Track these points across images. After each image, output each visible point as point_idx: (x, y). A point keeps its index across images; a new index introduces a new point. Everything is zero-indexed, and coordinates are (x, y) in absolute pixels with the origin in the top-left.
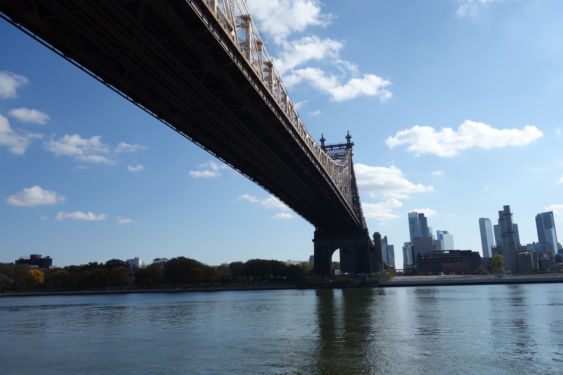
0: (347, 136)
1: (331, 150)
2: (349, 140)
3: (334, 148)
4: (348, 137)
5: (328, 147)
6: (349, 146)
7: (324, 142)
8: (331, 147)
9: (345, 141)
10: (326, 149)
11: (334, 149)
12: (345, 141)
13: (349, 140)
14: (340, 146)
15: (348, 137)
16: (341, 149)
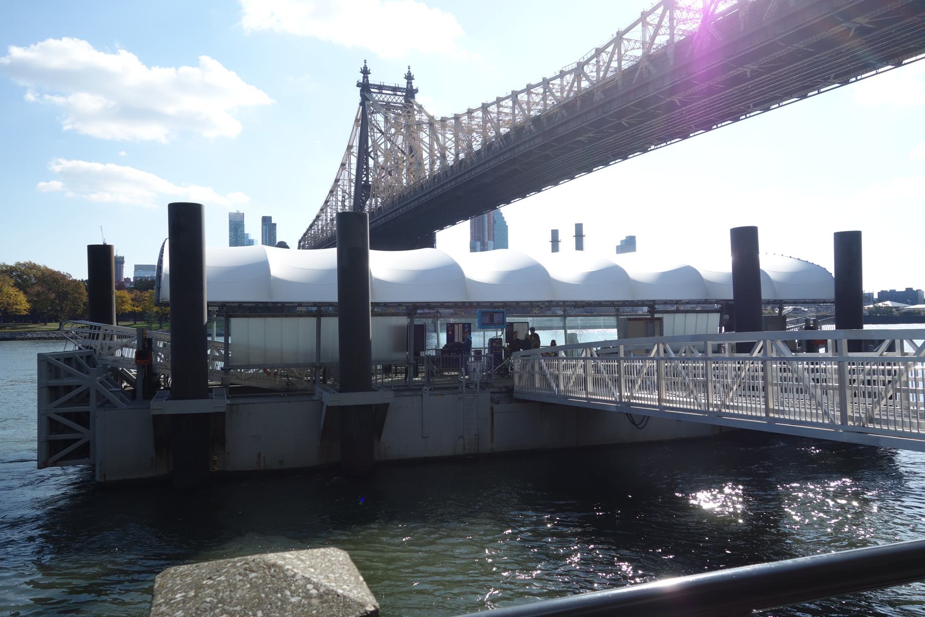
0: (407, 75)
1: (378, 93)
2: (409, 83)
3: (384, 91)
4: (409, 77)
5: (374, 86)
6: (410, 93)
7: (369, 75)
8: (381, 88)
9: (403, 84)
10: (372, 90)
11: (385, 94)
12: (403, 84)
13: (409, 83)
14: (395, 89)
15: (409, 77)
16: (396, 95)
